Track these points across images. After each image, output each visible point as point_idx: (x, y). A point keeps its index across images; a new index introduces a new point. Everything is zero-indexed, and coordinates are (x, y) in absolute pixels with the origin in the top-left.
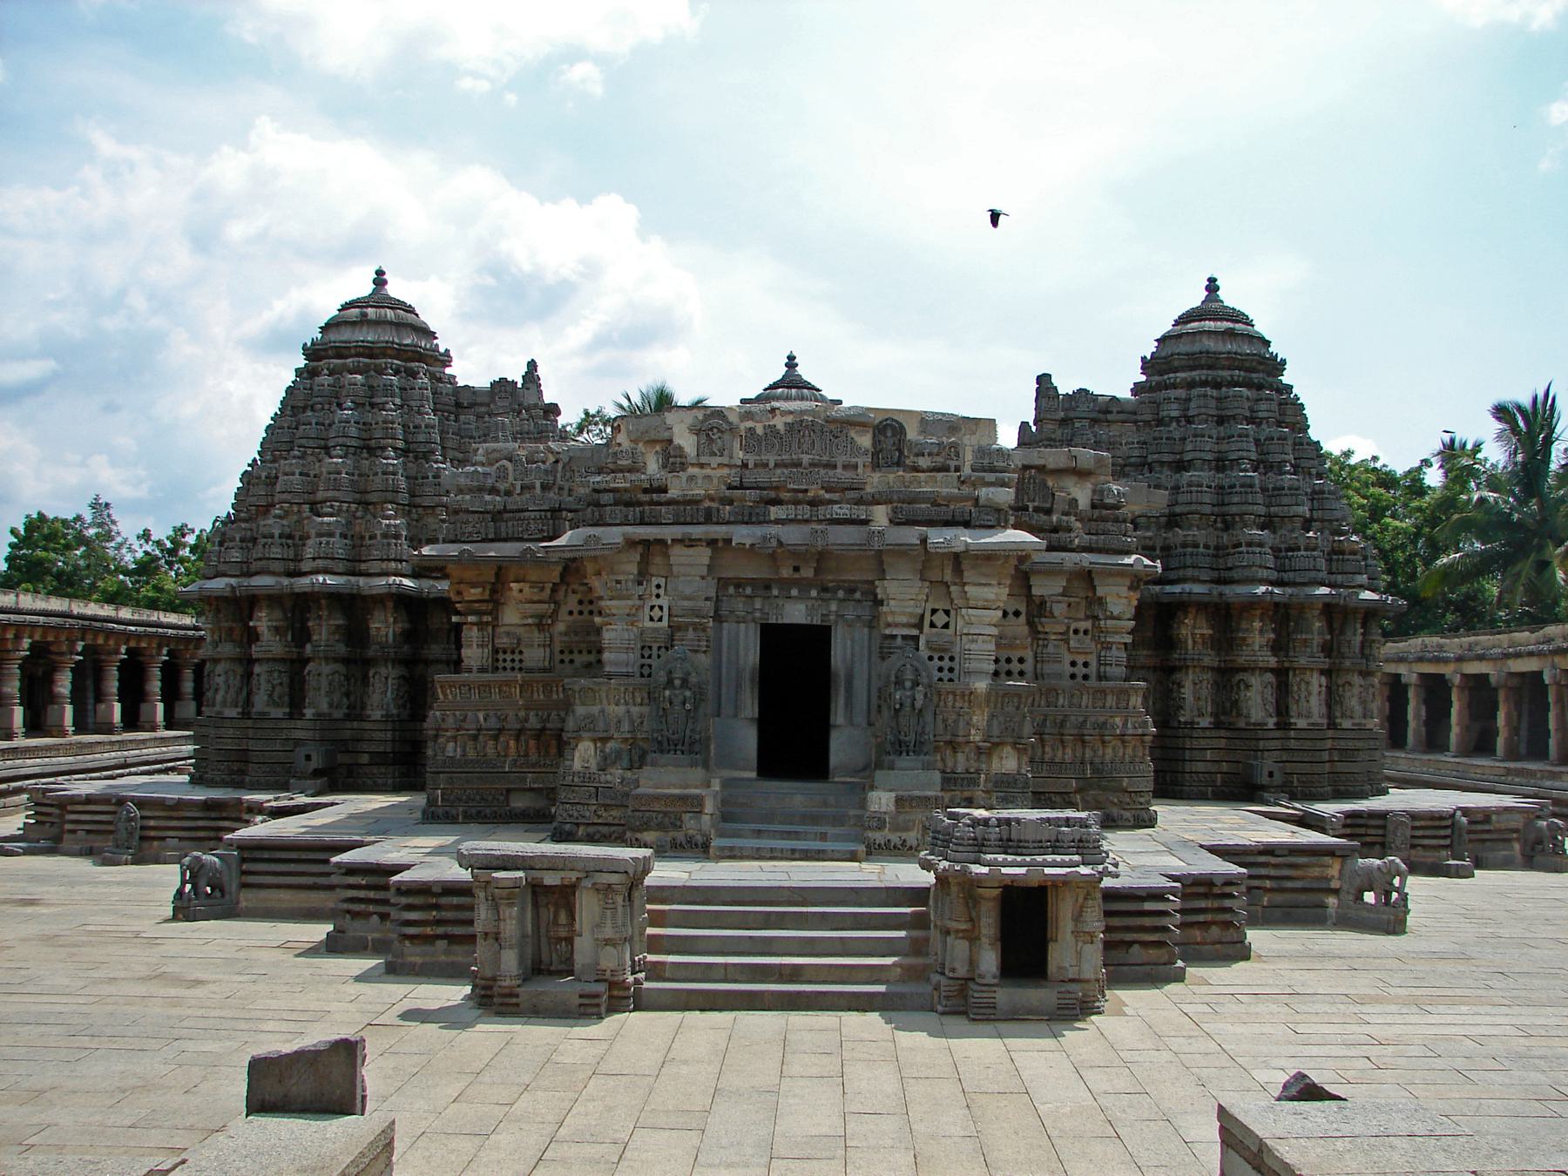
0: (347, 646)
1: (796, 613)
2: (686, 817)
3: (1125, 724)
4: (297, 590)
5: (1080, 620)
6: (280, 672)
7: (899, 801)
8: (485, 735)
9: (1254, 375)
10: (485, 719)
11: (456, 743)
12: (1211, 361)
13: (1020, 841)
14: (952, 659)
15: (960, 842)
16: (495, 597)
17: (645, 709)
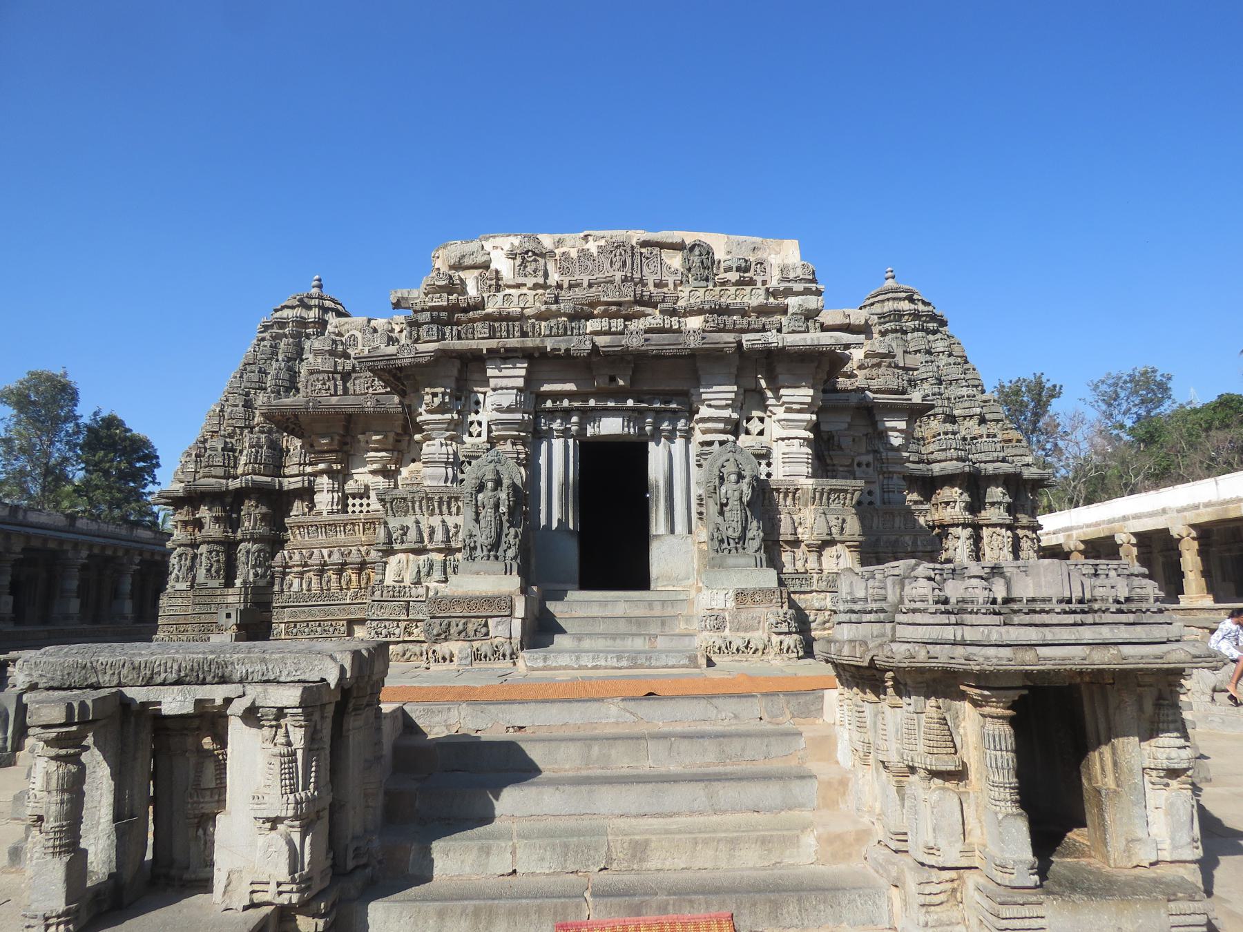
0: (271, 530)
1: (611, 426)
2: (489, 620)
3: (915, 542)
4: (230, 488)
5: (862, 454)
6: (218, 552)
7: (740, 595)
8: (329, 570)
9: (932, 324)
10: (329, 556)
11: (302, 579)
12: (898, 315)
13: (1033, 600)
14: (769, 465)
15: (919, 605)
16: (346, 448)
17: (459, 520)
